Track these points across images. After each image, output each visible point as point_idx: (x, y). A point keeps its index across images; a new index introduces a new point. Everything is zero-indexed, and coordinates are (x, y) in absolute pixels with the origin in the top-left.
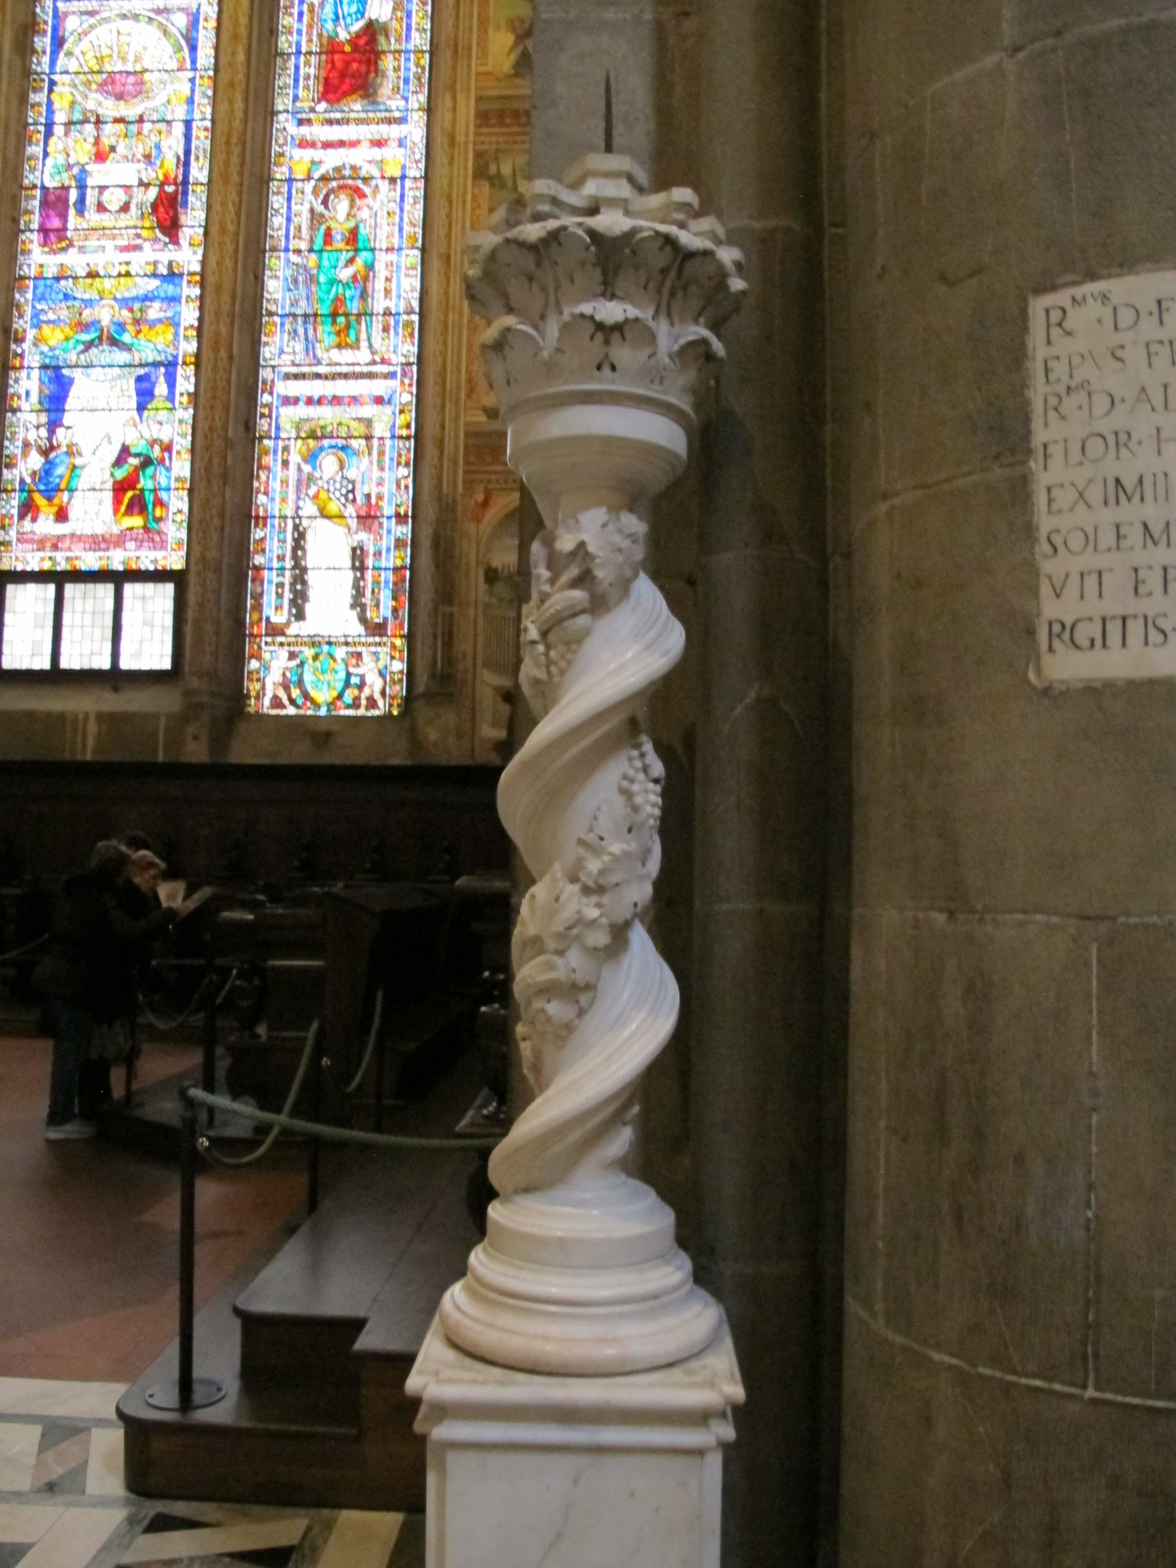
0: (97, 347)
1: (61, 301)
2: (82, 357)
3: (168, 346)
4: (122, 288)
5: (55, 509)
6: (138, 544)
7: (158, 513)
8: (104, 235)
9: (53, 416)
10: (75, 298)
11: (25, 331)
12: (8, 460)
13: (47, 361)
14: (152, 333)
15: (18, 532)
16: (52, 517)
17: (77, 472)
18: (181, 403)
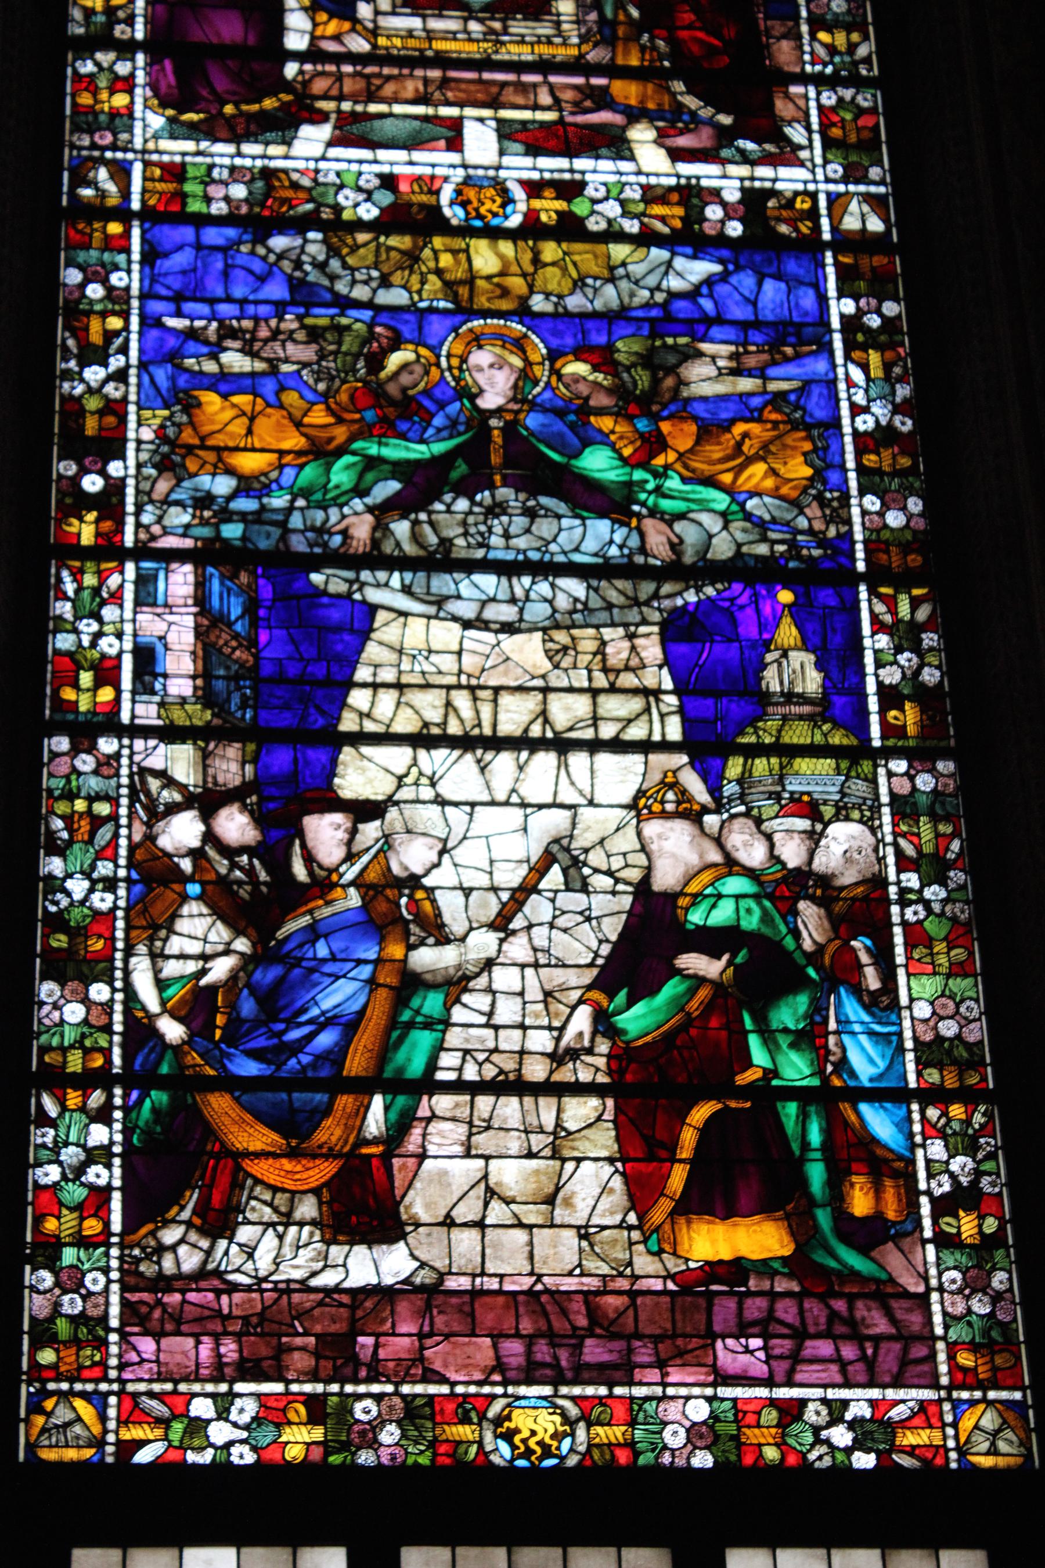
0: (466, 489)
1: (280, 308)
2: (401, 528)
3: (797, 505)
4: (551, 279)
5: (322, 1171)
6: (782, 1346)
7: (860, 1204)
8: (445, 83)
9: (281, 758)
10: (346, 303)
11: (116, 409)
12: (59, 941)
13: (232, 531)
14: (716, 452)
15: (131, 1280)
16: (307, 1208)
17: (432, 1003)
18: (900, 731)
